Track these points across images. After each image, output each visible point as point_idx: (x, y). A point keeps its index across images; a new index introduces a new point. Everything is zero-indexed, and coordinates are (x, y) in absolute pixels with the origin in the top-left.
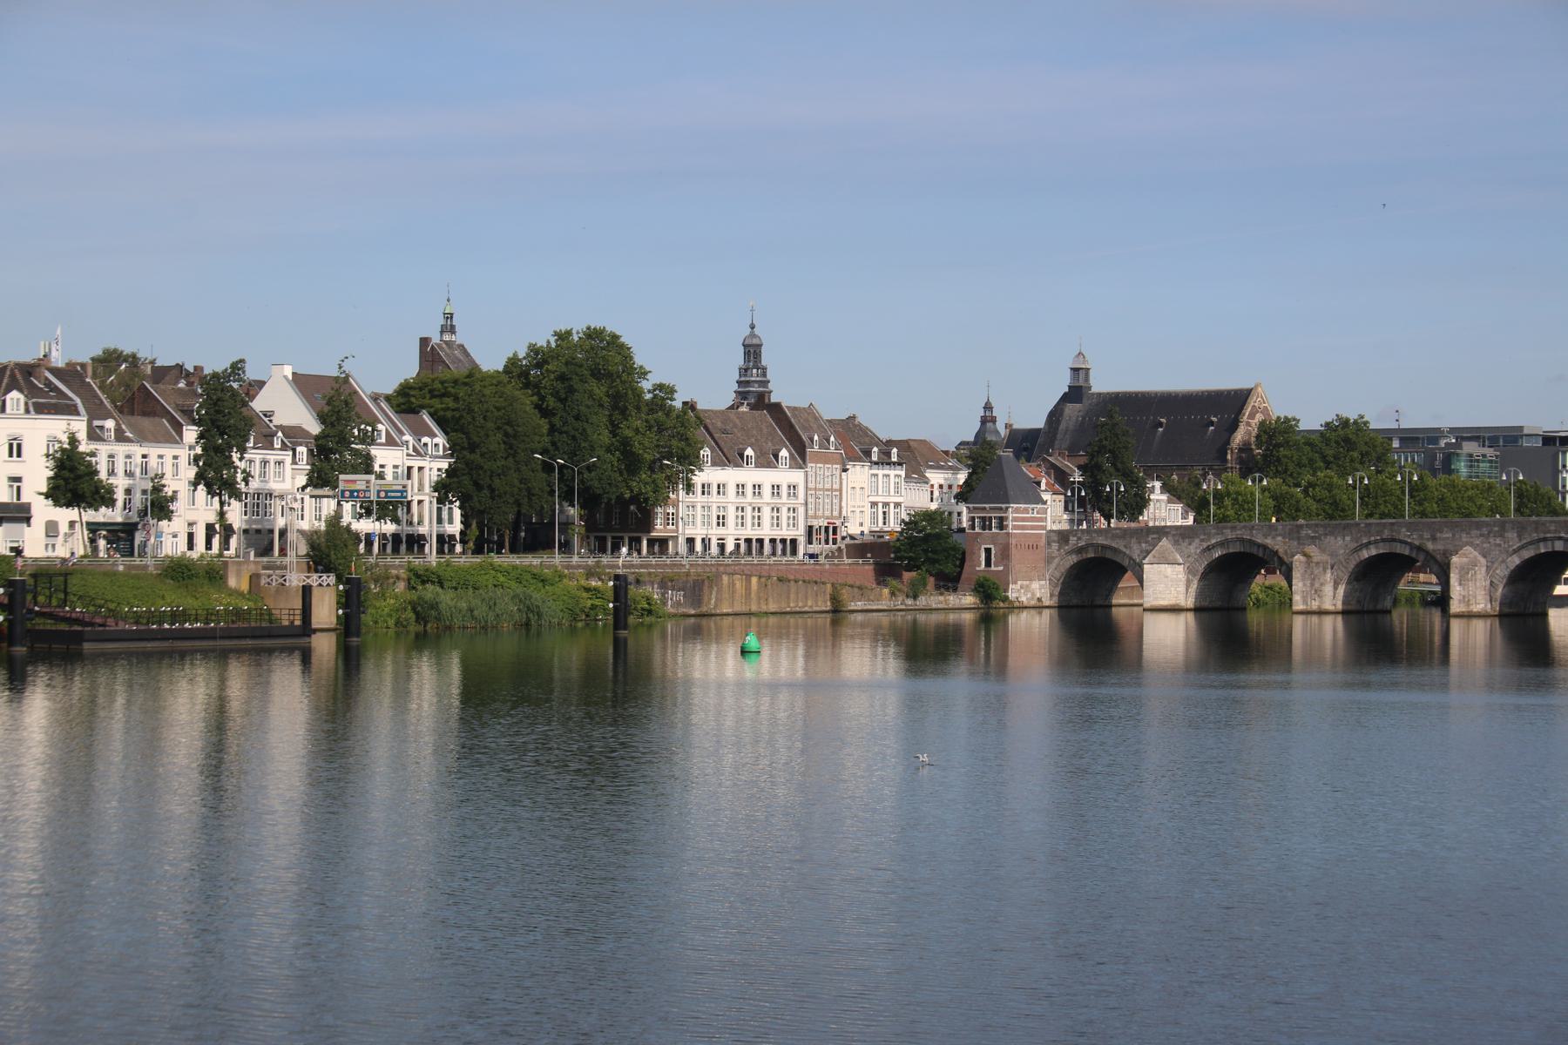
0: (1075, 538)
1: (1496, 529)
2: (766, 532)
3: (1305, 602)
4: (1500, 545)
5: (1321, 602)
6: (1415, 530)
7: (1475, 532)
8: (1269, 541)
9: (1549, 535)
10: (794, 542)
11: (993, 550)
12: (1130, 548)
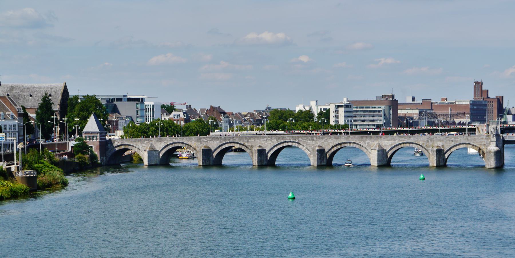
0: (117, 142)
1: (269, 139)
3: (206, 163)
4: (271, 144)
6: (241, 139)
7: (262, 140)
9: (287, 141)
11: (93, 147)
12: (138, 145)
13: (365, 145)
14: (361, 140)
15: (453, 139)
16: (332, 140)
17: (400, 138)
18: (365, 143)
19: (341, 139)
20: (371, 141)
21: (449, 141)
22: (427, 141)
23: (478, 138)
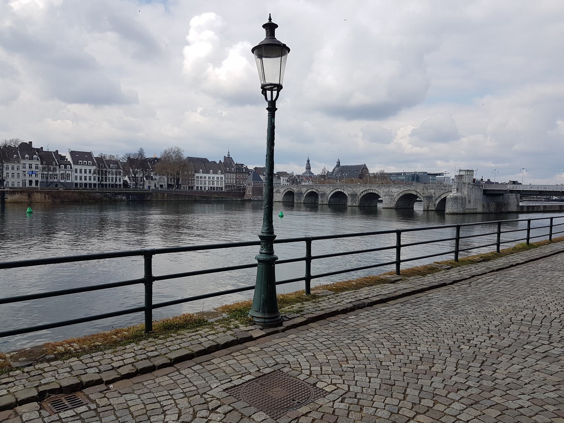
2: (215, 185)
5: (301, 201)
7: (326, 187)
8: (294, 189)
10: (222, 188)
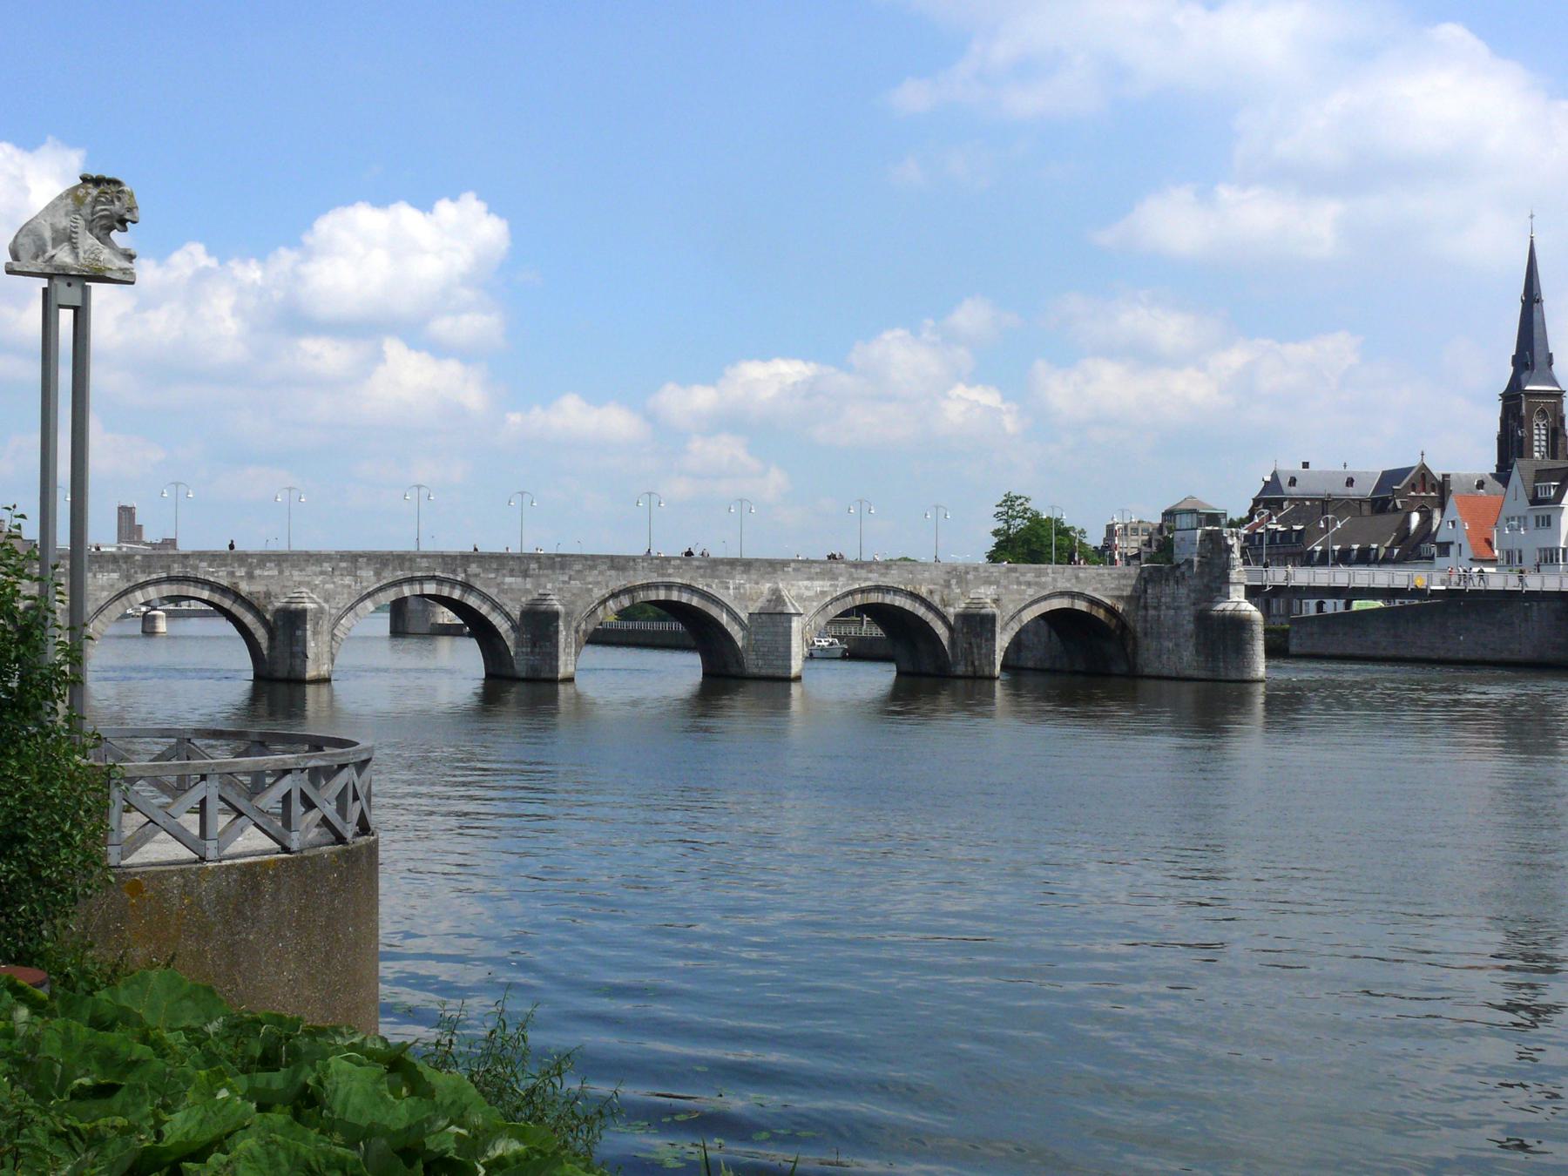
1: (343, 565)
4: (350, 586)
6: (225, 566)
9: (419, 574)
13: (727, 596)
14: (713, 577)
15: (1030, 577)
16: (601, 573)
17: (853, 570)
18: (728, 588)
19: (635, 570)
20: (749, 580)
21: (1019, 583)
22: (945, 581)
23: (1109, 574)
